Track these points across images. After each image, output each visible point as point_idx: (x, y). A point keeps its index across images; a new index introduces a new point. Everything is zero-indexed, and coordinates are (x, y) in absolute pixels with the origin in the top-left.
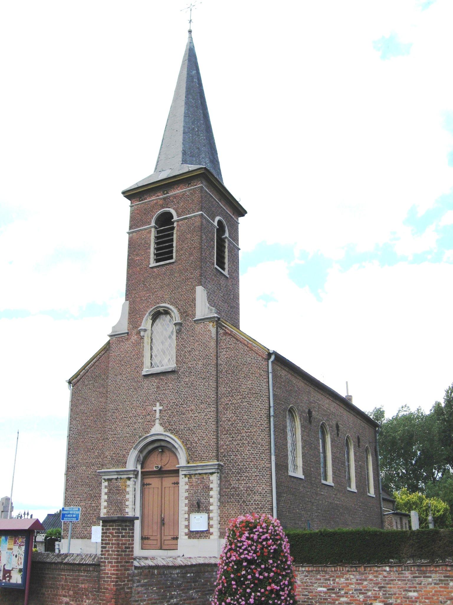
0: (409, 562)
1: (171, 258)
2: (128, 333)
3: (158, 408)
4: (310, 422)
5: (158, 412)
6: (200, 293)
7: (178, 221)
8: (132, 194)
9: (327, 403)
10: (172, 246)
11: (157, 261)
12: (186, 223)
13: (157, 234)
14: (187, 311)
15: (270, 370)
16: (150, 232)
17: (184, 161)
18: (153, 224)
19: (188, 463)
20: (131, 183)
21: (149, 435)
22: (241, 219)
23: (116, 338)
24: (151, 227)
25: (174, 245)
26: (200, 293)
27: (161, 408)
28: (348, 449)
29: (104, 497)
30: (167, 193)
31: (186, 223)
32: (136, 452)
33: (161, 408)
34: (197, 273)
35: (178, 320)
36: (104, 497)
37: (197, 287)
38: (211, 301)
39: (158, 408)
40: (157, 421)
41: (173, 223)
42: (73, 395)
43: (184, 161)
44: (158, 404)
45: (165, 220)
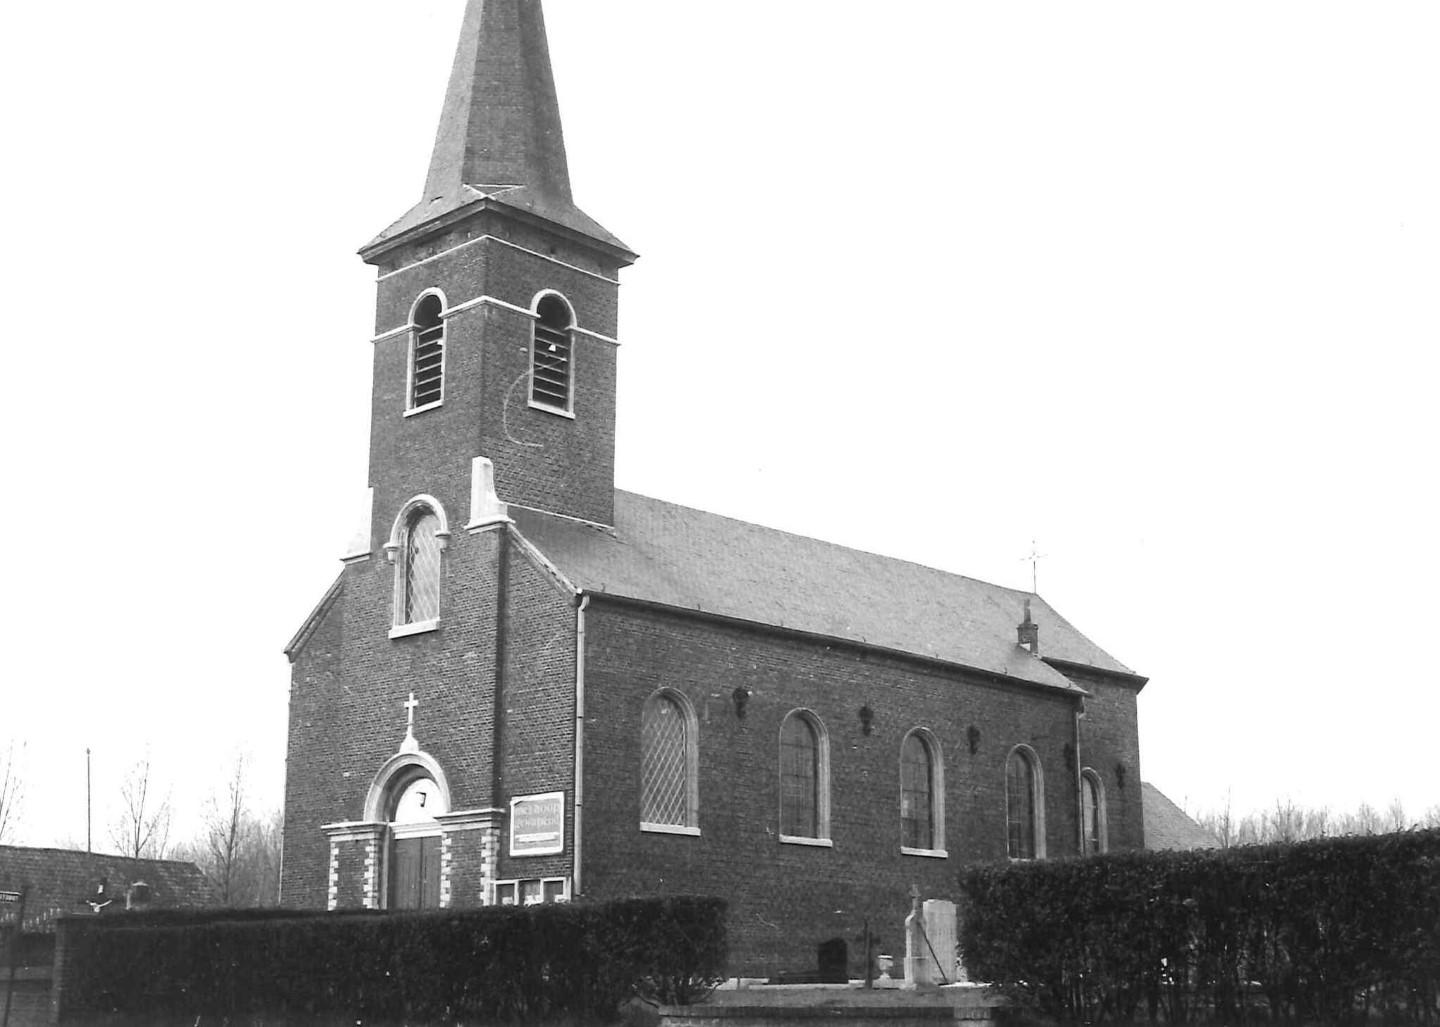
0: (10, 898)
1: (436, 397)
2: (369, 554)
3: (412, 703)
4: (740, 714)
5: (411, 711)
6: (481, 470)
7: (449, 316)
8: (383, 255)
9: (807, 667)
10: (437, 371)
11: (420, 402)
12: (505, 297)
13: (421, 342)
14: (458, 512)
15: (581, 627)
16: (407, 340)
17: (468, 177)
18: (411, 324)
19: (453, 811)
20: (368, 237)
21: (395, 756)
22: (622, 272)
23: (356, 566)
24: (408, 331)
25: (443, 370)
26: (481, 470)
27: (416, 703)
28: (929, 759)
29: (333, 877)
30: (434, 253)
31: (505, 297)
32: (379, 790)
33: (416, 703)
34: (474, 432)
35: (444, 530)
36: (333, 877)
37: (474, 460)
38: (501, 488)
39: (412, 703)
40: (410, 729)
41: (441, 321)
42: (296, 675)
43: (468, 177)
44: (411, 695)
45: (429, 311)
